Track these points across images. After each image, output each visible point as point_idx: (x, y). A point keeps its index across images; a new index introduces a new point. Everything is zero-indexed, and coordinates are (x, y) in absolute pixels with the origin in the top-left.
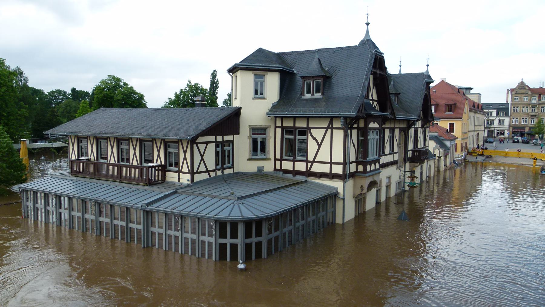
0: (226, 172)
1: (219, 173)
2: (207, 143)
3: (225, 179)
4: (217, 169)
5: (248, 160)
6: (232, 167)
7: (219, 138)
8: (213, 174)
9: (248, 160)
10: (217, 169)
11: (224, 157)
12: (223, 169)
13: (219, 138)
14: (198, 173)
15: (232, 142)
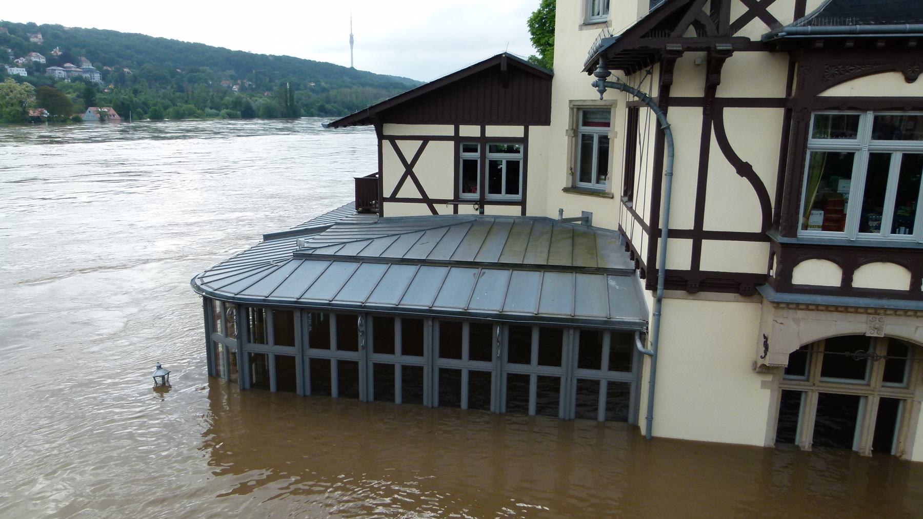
0: (490, 210)
1: (467, 210)
2: (426, 140)
3: (480, 227)
4: (456, 201)
5: (566, 190)
6: (523, 203)
7: (470, 131)
8: (445, 210)
9: (566, 190)
10: (456, 201)
11: (492, 175)
12: (481, 203)
13: (470, 131)
14: (393, 199)
15: (524, 140)
